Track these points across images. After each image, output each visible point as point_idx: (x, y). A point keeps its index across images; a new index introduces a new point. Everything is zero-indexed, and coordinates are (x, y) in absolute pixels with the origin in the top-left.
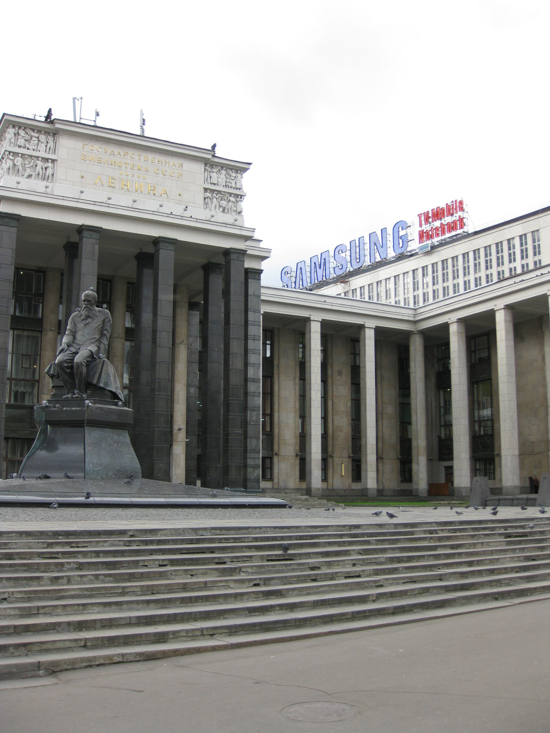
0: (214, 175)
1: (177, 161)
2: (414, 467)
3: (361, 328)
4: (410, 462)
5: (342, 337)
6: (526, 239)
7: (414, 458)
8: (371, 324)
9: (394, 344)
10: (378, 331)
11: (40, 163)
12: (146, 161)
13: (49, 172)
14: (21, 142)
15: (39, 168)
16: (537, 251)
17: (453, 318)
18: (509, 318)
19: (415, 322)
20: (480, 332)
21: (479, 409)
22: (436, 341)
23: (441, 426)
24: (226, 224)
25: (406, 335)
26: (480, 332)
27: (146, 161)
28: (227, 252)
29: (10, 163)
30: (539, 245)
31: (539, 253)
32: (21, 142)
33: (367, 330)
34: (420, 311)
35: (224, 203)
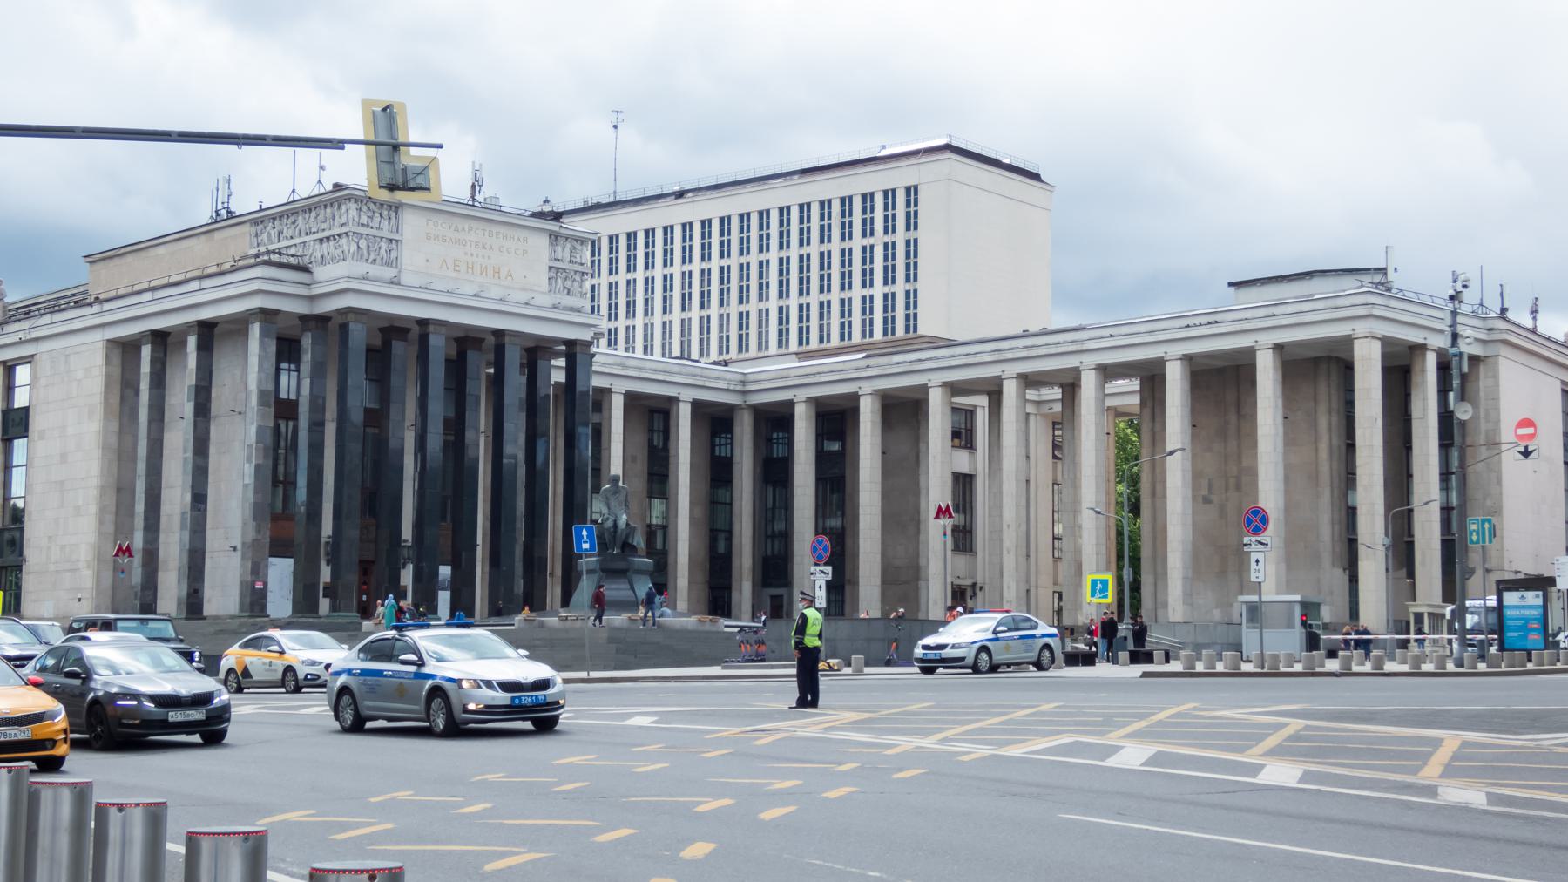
0: (559, 249)
1: (525, 233)
2: (735, 595)
3: (674, 400)
4: (729, 588)
5: (652, 414)
6: (894, 196)
7: (735, 585)
8: (687, 395)
9: (714, 421)
10: (697, 405)
11: (384, 245)
12: (491, 235)
13: (394, 254)
14: (364, 219)
15: (383, 252)
16: (912, 222)
17: (800, 396)
18: (878, 406)
19: (744, 393)
20: (836, 419)
21: (824, 517)
22: (774, 420)
23: (767, 537)
24: (572, 309)
25: (731, 409)
26: (836, 419)
27: (491, 235)
28: (570, 344)
29: (353, 247)
30: (916, 212)
31: (916, 228)
32: (364, 219)
33: (682, 405)
34: (751, 378)
35: (568, 284)
